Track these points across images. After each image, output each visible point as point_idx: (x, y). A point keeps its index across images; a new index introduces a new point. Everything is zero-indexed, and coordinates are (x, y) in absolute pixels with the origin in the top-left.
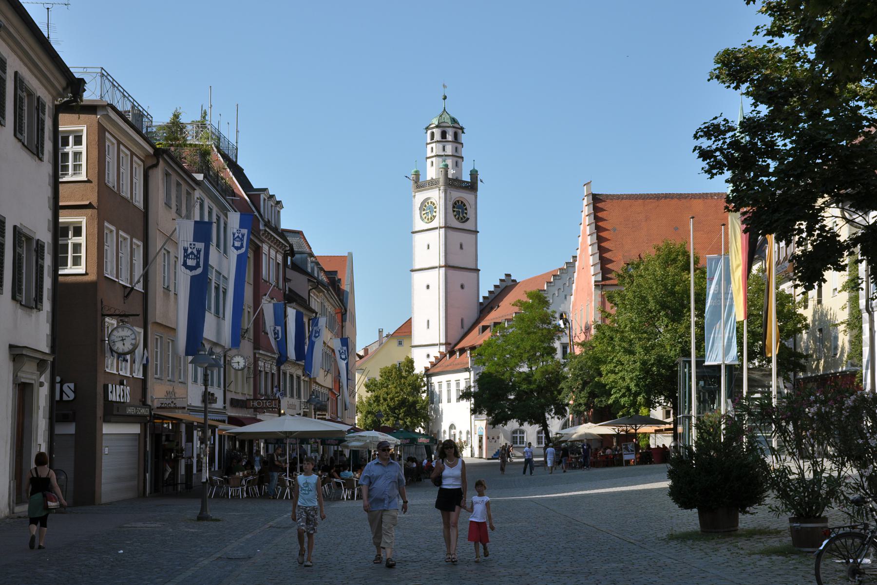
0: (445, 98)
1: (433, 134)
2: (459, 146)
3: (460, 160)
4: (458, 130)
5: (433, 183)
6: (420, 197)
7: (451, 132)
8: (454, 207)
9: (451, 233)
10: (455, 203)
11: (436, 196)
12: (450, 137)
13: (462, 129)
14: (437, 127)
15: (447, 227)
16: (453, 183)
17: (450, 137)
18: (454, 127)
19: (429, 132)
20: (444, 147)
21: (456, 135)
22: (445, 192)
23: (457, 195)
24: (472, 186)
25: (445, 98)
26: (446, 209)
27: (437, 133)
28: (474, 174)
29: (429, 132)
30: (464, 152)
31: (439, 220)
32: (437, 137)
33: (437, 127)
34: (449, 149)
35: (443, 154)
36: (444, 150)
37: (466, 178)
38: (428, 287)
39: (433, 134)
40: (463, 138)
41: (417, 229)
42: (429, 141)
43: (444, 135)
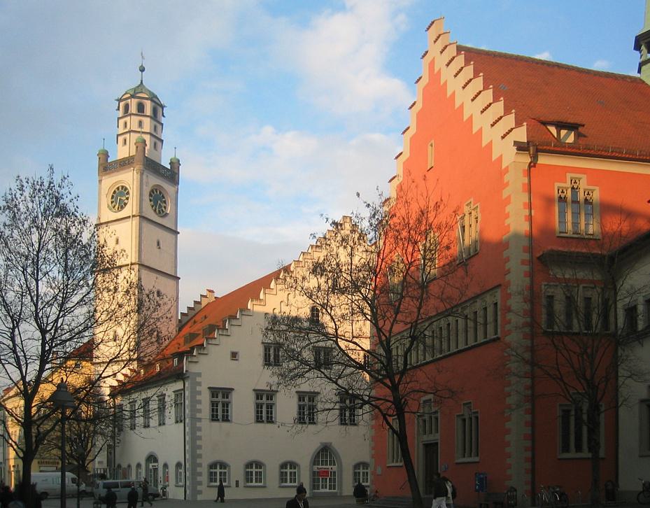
2: (159, 127)
3: (159, 143)
4: (158, 107)
5: (124, 164)
6: (110, 181)
8: (150, 195)
9: (145, 224)
10: (152, 191)
11: (129, 178)
13: (162, 107)
17: (148, 111)
18: (152, 101)
19: (122, 104)
21: (155, 111)
22: (142, 174)
23: (154, 181)
24: (172, 174)
25: (142, 70)
26: (141, 195)
30: (166, 135)
31: (131, 208)
32: (133, 109)
35: (139, 130)
37: (166, 163)
42: (121, 113)
43: (141, 108)
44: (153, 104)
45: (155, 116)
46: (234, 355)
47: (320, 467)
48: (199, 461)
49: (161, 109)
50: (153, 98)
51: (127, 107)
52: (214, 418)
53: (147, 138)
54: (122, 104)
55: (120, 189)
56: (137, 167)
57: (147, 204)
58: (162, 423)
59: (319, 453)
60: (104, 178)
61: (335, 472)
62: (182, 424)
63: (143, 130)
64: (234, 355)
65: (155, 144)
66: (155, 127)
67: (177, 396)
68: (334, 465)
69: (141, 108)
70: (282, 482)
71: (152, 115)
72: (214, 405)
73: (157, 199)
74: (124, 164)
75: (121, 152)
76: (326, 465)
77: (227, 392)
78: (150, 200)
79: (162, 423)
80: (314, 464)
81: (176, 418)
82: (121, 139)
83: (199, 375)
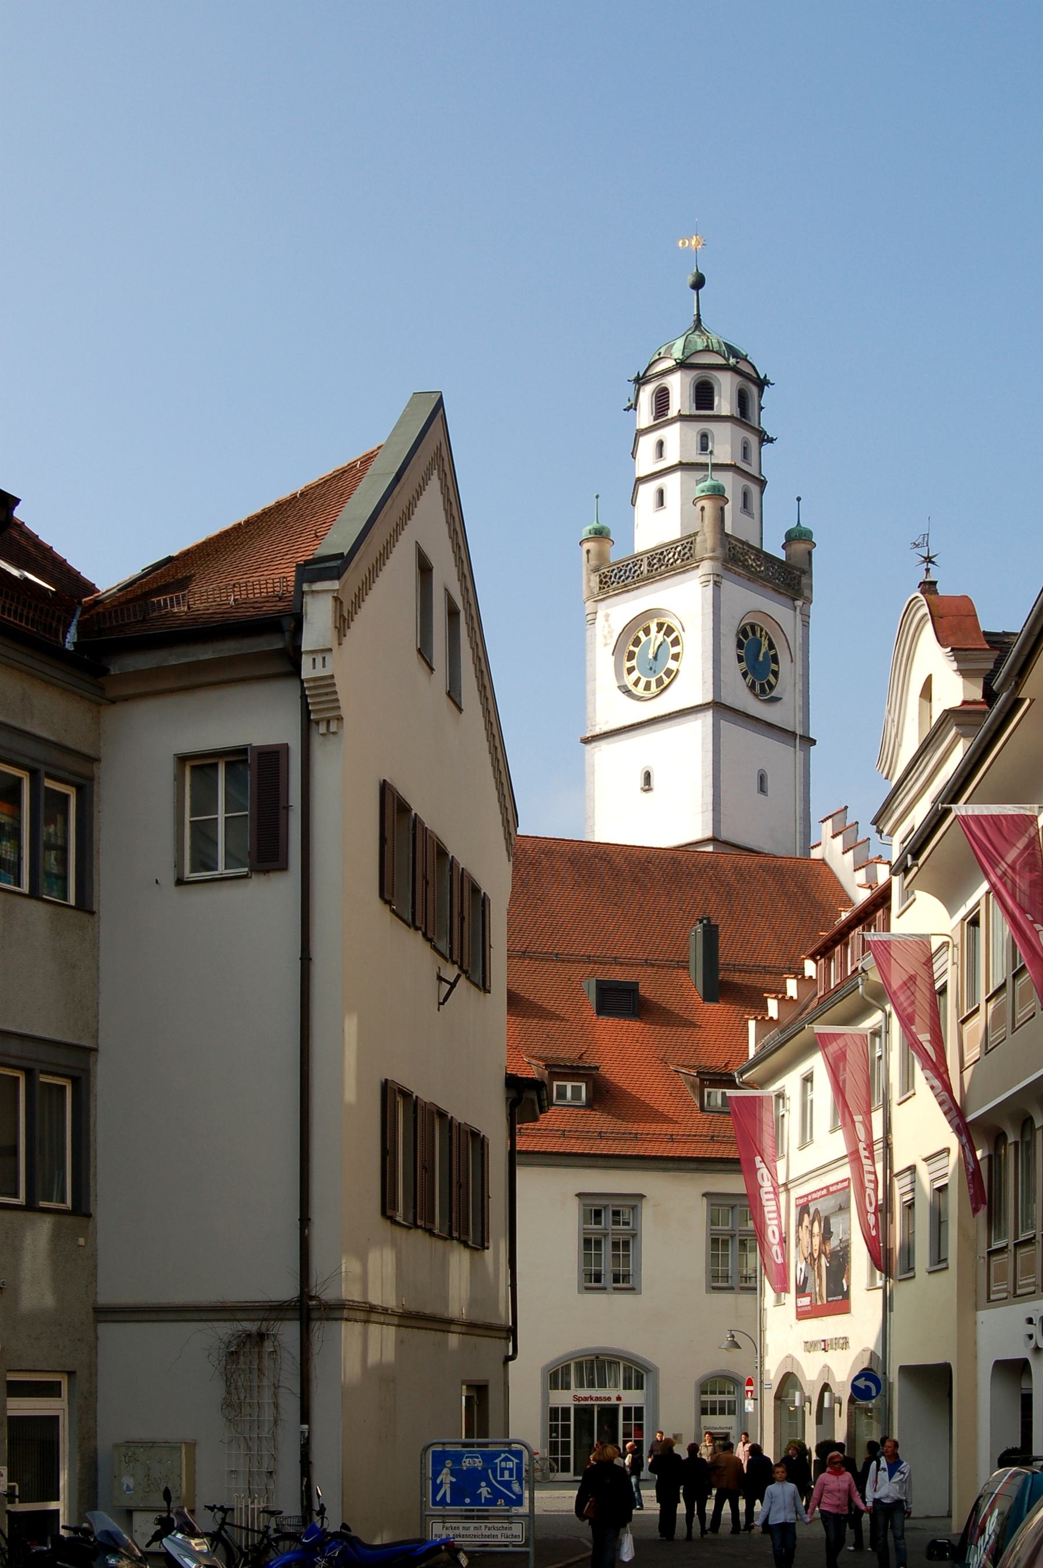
0: (699, 283)
1: (662, 398)
4: (753, 384)
5: (663, 563)
6: (619, 612)
7: (727, 388)
8: (740, 645)
10: (743, 632)
12: (724, 403)
13: (762, 384)
14: (682, 365)
15: (719, 707)
16: (738, 559)
17: (724, 403)
18: (735, 370)
19: (647, 393)
20: (704, 437)
21: (742, 400)
23: (749, 600)
25: (699, 283)
27: (679, 387)
28: (798, 537)
29: (647, 393)
31: (693, 683)
33: (682, 365)
34: (723, 451)
36: (704, 447)
37: (774, 546)
39: (662, 398)
40: (771, 413)
41: (597, 731)
42: (645, 416)
43: (704, 395)
44: (738, 379)
45: (744, 411)
49: (754, 390)
50: (735, 361)
53: (727, 480)
56: (706, 567)
57: (733, 669)
65: (746, 495)
66: (746, 450)
71: (736, 413)
73: (755, 657)
74: (663, 563)
75: (655, 526)
78: (740, 659)
82: (647, 492)
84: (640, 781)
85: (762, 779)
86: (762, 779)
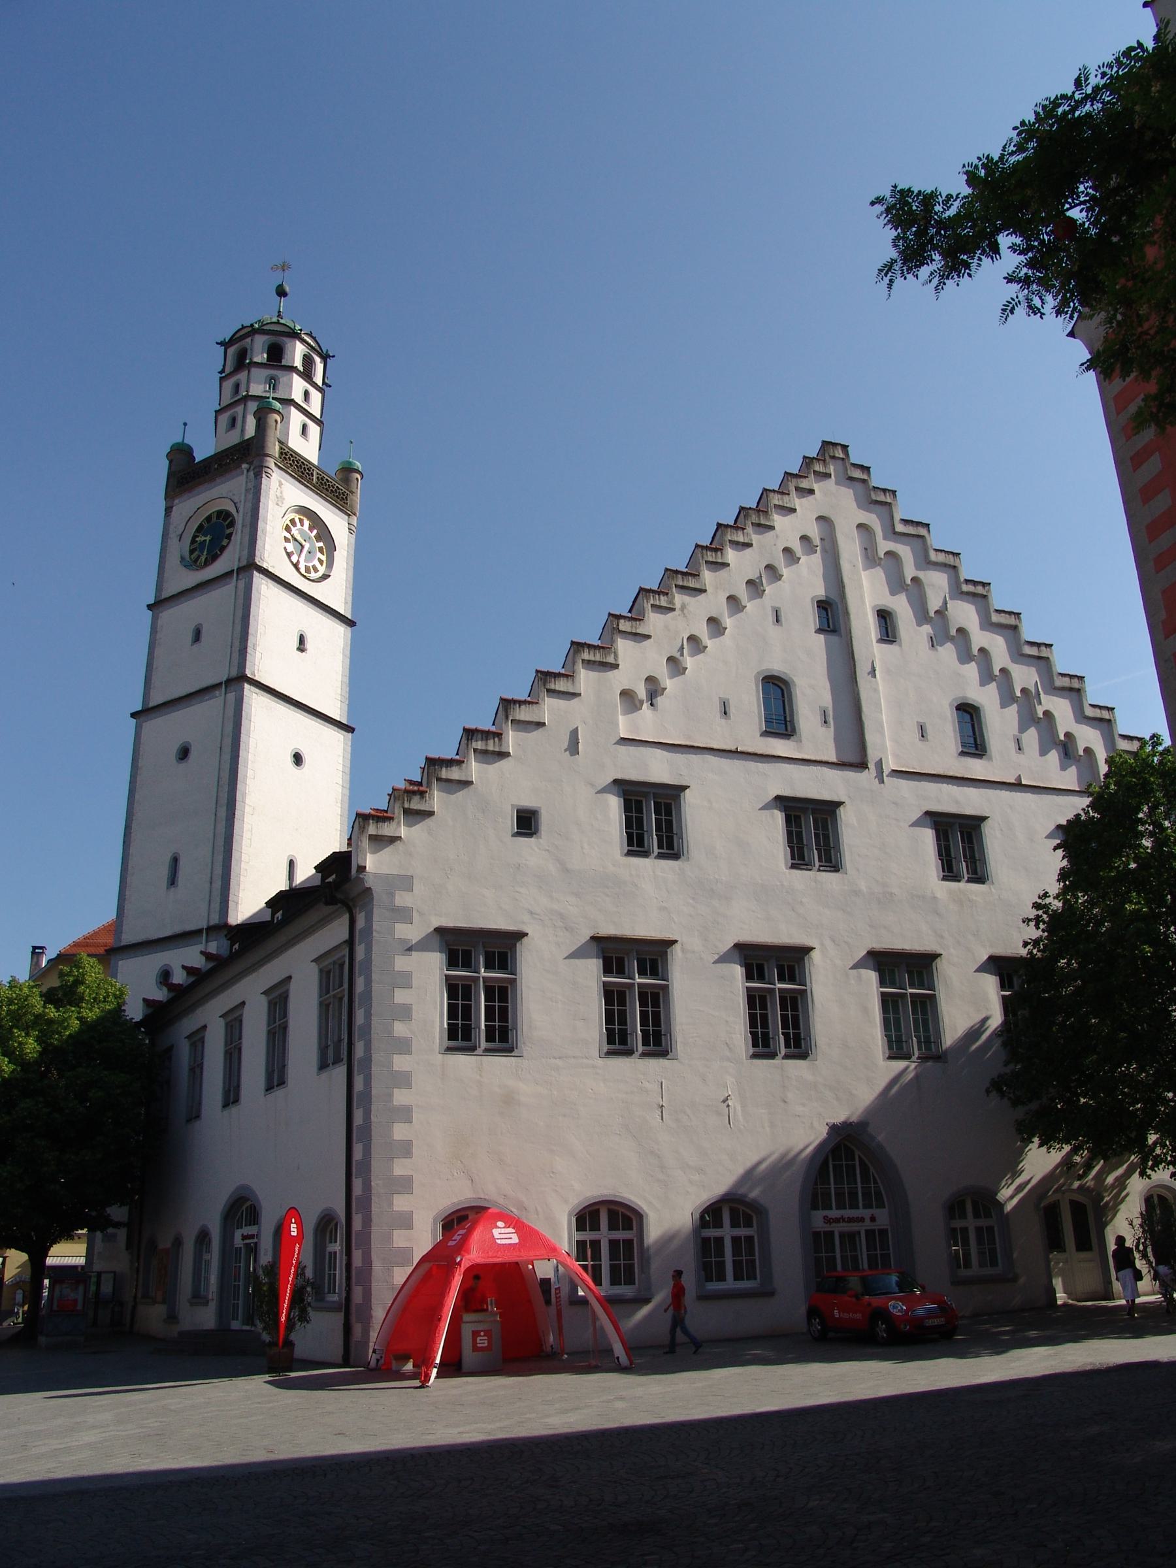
19: (232, 351)
21: (308, 361)
38: (184, 753)
46: (527, 822)
47: (834, 1213)
48: (401, 1203)
51: (242, 355)
52: (459, 1035)
54: (232, 351)
55: (214, 519)
58: (276, 1078)
59: (825, 1163)
60: (176, 501)
61: (883, 1233)
62: (340, 1071)
63: (276, 396)
64: (527, 822)
65: (304, 427)
67: (325, 974)
68: (881, 1205)
69: (276, 354)
70: (709, 1279)
72: (458, 992)
76: (854, 1206)
77: (501, 948)
79: (276, 1078)
80: (815, 1207)
81: (323, 1050)
83: (406, 882)
84: (190, 636)
85: (302, 640)
86: (302, 640)
